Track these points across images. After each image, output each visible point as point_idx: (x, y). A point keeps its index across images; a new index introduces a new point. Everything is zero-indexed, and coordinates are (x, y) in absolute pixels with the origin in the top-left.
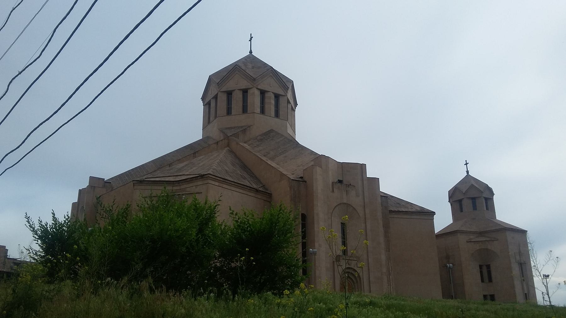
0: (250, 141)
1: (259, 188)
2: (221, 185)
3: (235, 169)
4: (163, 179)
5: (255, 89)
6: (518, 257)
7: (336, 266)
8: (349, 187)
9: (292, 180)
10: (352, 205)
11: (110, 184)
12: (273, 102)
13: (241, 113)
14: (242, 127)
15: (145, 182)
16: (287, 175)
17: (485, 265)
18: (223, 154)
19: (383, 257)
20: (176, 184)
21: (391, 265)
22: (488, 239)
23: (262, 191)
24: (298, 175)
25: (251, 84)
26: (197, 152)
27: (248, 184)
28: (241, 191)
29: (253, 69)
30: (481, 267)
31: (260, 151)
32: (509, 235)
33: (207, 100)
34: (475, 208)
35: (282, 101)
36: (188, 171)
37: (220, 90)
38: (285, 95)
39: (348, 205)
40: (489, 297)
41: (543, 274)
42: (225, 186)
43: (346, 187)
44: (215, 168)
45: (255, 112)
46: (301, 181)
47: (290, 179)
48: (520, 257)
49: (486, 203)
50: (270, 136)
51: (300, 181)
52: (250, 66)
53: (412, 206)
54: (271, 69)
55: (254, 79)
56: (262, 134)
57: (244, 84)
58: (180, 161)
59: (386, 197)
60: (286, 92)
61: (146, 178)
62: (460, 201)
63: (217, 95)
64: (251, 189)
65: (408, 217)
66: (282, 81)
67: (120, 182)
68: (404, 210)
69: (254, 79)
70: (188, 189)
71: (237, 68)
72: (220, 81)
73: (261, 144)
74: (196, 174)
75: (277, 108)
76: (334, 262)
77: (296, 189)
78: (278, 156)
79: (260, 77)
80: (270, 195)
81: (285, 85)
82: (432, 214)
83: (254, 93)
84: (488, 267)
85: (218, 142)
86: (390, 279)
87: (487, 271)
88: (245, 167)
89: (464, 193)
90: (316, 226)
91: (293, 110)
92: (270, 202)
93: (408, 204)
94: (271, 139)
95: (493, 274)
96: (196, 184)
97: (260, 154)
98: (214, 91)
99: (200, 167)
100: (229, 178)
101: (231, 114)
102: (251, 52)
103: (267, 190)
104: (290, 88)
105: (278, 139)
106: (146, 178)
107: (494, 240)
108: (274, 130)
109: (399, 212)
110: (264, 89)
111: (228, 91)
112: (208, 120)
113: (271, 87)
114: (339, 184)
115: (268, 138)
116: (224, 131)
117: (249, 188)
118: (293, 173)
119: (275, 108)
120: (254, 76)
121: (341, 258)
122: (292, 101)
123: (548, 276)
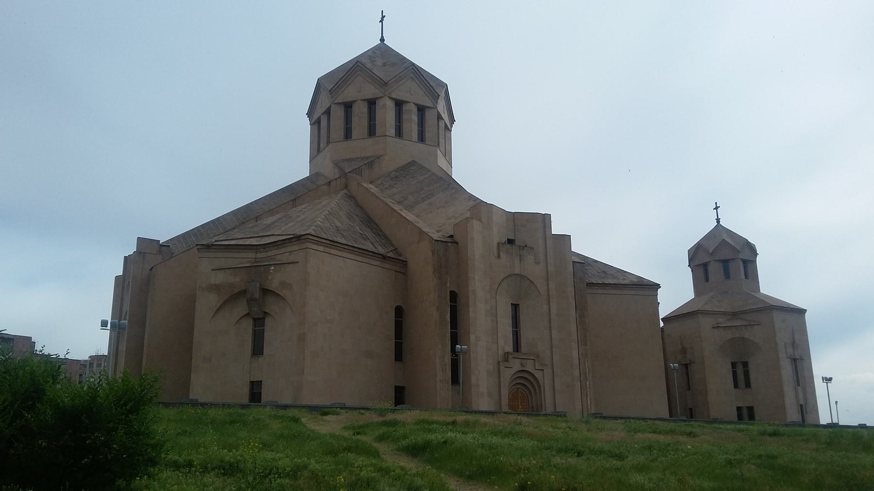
0: (380, 180)
1: (387, 253)
2: (327, 250)
3: (351, 224)
4: (241, 242)
6: (790, 351)
7: (502, 367)
8: (524, 249)
9: (436, 240)
10: (528, 277)
11: (168, 248)
12: (415, 118)
13: (366, 137)
14: (368, 158)
15: (215, 247)
16: (429, 232)
17: (741, 362)
18: (336, 202)
19: (575, 354)
20: (262, 250)
22: (744, 323)
23: (392, 258)
24: (448, 233)
25: (380, 91)
26: (299, 197)
27: (370, 247)
28: (359, 258)
29: (384, 68)
30: (734, 365)
31: (394, 194)
32: (777, 317)
33: (316, 117)
34: (727, 275)
35: (430, 116)
36: (279, 229)
37: (334, 100)
38: (435, 107)
39: (522, 277)
40: (745, 412)
41: (823, 377)
42: (333, 251)
44: (320, 223)
45: (388, 134)
46: (450, 242)
47: (433, 239)
48: (794, 351)
49: (745, 268)
50: (410, 172)
51: (448, 242)
52: (379, 62)
53: (625, 276)
54: (412, 67)
55: (386, 84)
56: (398, 168)
57: (370, 91)
58: (272, 212)
59: (582, 263)
60: (435, 104)
61: (216, 241)
62: (705, 266)
63: (329, 109)
64: (375, 255)
65: (619, 292)
66: (428, 84)
67: (184, 244)
68: (612, 283)
69: (386, 83)
70: (279, 257)
71: (358, 67)
72: (333, 87)
73: (396, 184)
74: (290, 235)
75: (422, 128)
76: (499, 362)
77: (441, 255)
78: (419, 203)
80: (404, 263)
81: (433, 91)
82: (654, 287)
83: (385, 105)
84: (745, 365)
85: (330, 182)
86: (586, 385)
87: (744, 371)
88: (369, 222)
89: (711, 254)
90: (471, 309)
91: (448, 129)
92: (405, 273)
93: (620, 272)
94: (411, 176)
95: (753, 376)
96: (289, 249)
97: (392, 201)
98: (325, 102)
99: (300, 222)
100: (339, 239)
101: (351, 138)
102: (382, 40)
103: (400, 255)
104: (442, 95)
105: (421, 176)
106: (216, 241)
107: (756, 325)
108: (417, 163)
110: (401, 99)
112: (317, 149)
113: (412, 95)
114: (509, 246)
115: (408, 175)
116: (340, 164)
117: (371, 254)
118: (440, 229)
119: (418, 126)
120: (386, 79)
121: (510, 357)
122: (445, 116)
123: (830, 379)
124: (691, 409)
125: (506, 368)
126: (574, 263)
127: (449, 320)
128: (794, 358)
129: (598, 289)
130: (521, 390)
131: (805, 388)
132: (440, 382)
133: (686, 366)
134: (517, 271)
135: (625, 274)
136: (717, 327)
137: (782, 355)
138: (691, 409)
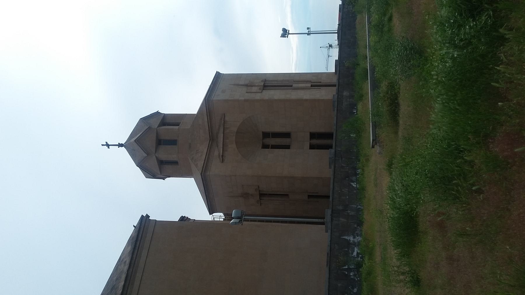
6: (254, 89)
34: (173, 142)
40: (315, 142)
62: (161, 163)
65: (139, 275)
68: (123, 283)
84: (266, 135)
89: (148, 154)
107: (224, 119)
124: (309, 196)
128: (262, 87)
131: (294, 81)
133: (262, 195)
135: (121, 259)
136: (223, 158)
137: (258, 96)
138: (309, 196)
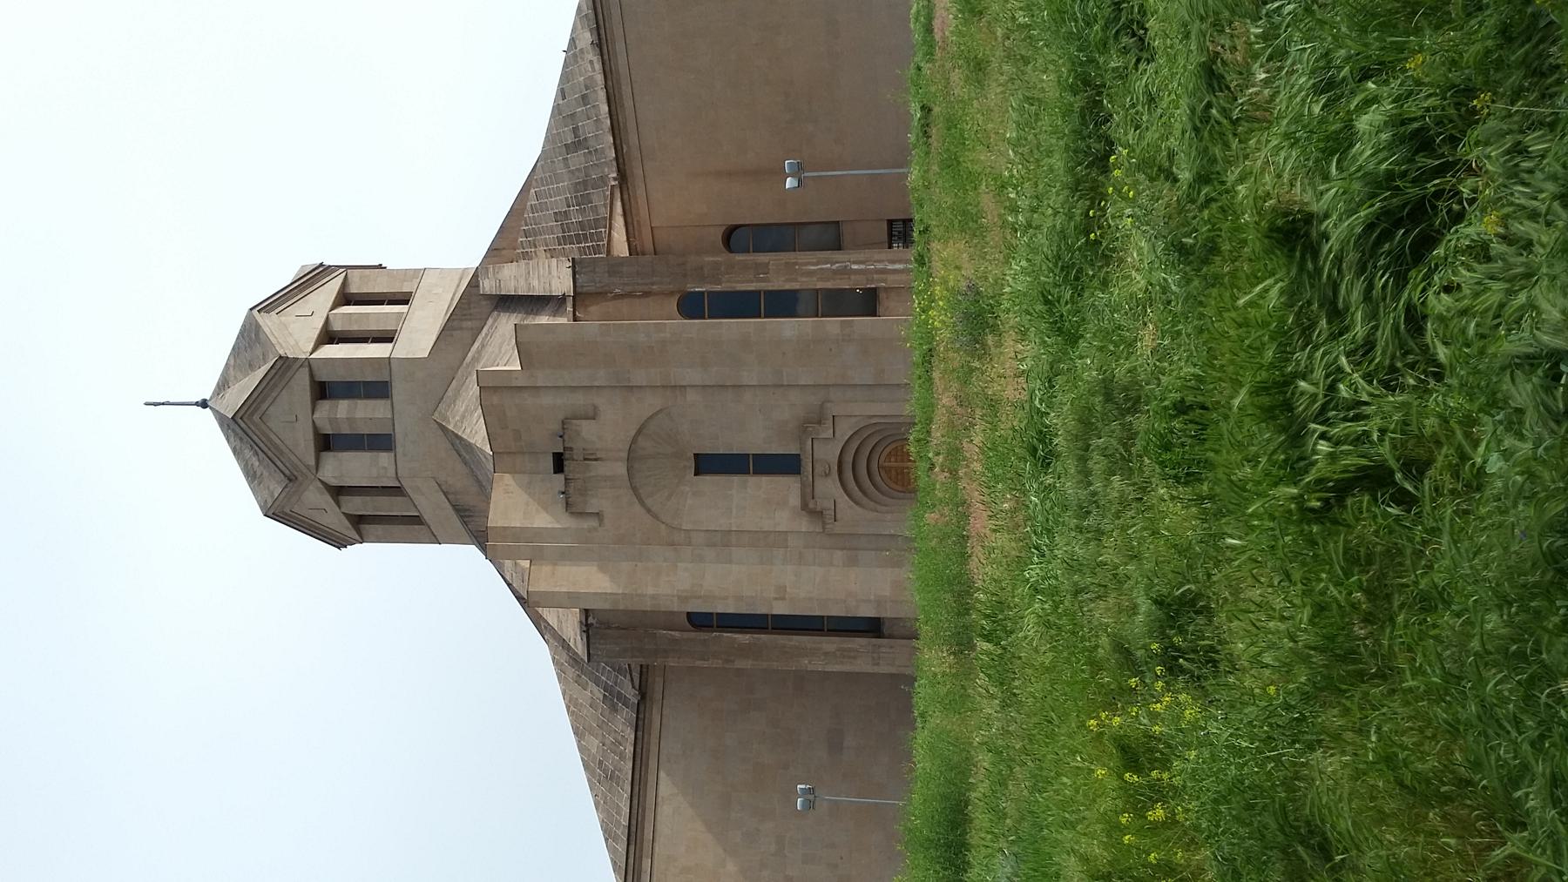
5: (320, 475)
7: (838, 528)
8: (571, 449)
10: (630, 439)
21: (813, 264)
38: (306, 363)
39: (632, 458)
43: (573, 460)
45: (392, 472)
55: (291, 479)
57: (314, 499)
65: (626, 90)
69: (290, 480)
79: (279, 463)
102: (204, 404)
109: (614, 129)
111: (353, 525)
117: (640, 733)
125: (838, 516)
126: (579, 290)
127: (748, 636)
129: (629, 147)
130: (882, 458)
132: (878, 664)
134: (621, 469)
